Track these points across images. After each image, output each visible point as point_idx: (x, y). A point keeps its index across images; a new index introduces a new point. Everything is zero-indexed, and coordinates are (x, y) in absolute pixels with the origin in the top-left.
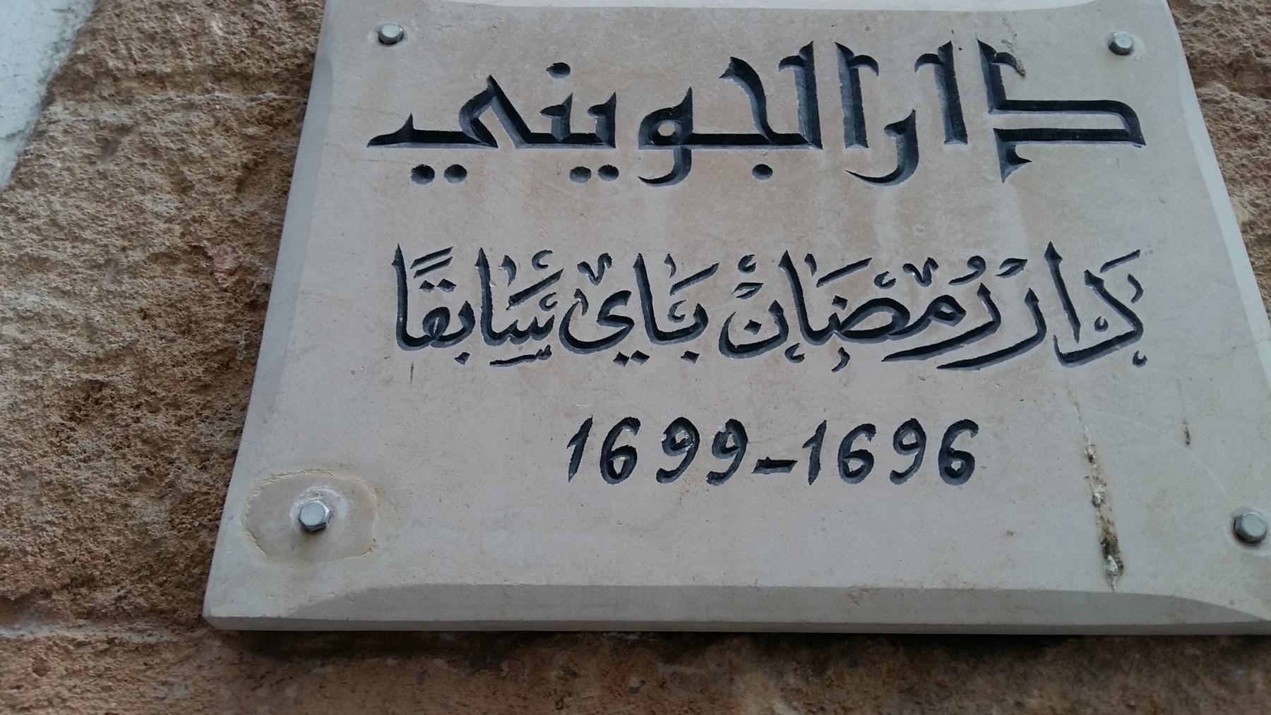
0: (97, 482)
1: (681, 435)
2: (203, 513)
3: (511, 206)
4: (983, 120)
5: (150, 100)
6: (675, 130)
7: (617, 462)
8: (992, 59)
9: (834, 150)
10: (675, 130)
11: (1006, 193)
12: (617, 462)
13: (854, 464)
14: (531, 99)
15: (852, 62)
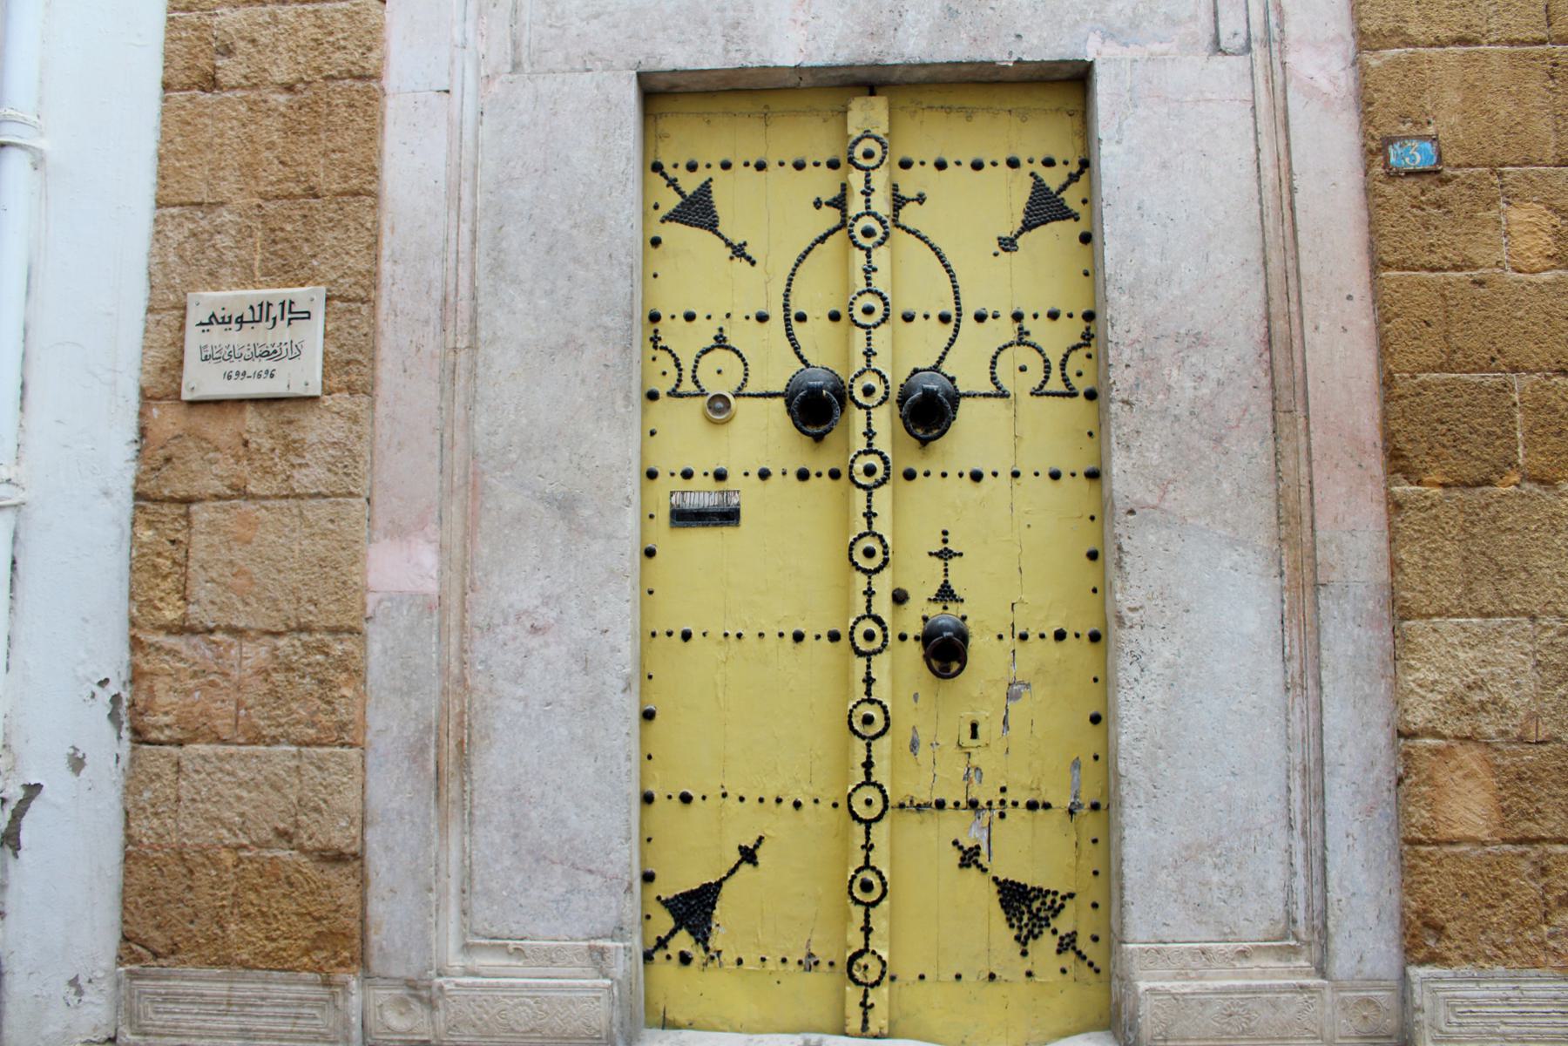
0: (167, 381)
1: (238, 373)
2: (180, 385)
3: (217, 336)
4: (287, 316)
5: (164, 314)
6: (241, 321)
7: (229, 377)
8: (292, 303)
9: (264, 324)
10: (241, 321)
11: (288, 330)
12: (229, 377)
13: (259, 376)
14: (219, 316)
15: (269, 305)
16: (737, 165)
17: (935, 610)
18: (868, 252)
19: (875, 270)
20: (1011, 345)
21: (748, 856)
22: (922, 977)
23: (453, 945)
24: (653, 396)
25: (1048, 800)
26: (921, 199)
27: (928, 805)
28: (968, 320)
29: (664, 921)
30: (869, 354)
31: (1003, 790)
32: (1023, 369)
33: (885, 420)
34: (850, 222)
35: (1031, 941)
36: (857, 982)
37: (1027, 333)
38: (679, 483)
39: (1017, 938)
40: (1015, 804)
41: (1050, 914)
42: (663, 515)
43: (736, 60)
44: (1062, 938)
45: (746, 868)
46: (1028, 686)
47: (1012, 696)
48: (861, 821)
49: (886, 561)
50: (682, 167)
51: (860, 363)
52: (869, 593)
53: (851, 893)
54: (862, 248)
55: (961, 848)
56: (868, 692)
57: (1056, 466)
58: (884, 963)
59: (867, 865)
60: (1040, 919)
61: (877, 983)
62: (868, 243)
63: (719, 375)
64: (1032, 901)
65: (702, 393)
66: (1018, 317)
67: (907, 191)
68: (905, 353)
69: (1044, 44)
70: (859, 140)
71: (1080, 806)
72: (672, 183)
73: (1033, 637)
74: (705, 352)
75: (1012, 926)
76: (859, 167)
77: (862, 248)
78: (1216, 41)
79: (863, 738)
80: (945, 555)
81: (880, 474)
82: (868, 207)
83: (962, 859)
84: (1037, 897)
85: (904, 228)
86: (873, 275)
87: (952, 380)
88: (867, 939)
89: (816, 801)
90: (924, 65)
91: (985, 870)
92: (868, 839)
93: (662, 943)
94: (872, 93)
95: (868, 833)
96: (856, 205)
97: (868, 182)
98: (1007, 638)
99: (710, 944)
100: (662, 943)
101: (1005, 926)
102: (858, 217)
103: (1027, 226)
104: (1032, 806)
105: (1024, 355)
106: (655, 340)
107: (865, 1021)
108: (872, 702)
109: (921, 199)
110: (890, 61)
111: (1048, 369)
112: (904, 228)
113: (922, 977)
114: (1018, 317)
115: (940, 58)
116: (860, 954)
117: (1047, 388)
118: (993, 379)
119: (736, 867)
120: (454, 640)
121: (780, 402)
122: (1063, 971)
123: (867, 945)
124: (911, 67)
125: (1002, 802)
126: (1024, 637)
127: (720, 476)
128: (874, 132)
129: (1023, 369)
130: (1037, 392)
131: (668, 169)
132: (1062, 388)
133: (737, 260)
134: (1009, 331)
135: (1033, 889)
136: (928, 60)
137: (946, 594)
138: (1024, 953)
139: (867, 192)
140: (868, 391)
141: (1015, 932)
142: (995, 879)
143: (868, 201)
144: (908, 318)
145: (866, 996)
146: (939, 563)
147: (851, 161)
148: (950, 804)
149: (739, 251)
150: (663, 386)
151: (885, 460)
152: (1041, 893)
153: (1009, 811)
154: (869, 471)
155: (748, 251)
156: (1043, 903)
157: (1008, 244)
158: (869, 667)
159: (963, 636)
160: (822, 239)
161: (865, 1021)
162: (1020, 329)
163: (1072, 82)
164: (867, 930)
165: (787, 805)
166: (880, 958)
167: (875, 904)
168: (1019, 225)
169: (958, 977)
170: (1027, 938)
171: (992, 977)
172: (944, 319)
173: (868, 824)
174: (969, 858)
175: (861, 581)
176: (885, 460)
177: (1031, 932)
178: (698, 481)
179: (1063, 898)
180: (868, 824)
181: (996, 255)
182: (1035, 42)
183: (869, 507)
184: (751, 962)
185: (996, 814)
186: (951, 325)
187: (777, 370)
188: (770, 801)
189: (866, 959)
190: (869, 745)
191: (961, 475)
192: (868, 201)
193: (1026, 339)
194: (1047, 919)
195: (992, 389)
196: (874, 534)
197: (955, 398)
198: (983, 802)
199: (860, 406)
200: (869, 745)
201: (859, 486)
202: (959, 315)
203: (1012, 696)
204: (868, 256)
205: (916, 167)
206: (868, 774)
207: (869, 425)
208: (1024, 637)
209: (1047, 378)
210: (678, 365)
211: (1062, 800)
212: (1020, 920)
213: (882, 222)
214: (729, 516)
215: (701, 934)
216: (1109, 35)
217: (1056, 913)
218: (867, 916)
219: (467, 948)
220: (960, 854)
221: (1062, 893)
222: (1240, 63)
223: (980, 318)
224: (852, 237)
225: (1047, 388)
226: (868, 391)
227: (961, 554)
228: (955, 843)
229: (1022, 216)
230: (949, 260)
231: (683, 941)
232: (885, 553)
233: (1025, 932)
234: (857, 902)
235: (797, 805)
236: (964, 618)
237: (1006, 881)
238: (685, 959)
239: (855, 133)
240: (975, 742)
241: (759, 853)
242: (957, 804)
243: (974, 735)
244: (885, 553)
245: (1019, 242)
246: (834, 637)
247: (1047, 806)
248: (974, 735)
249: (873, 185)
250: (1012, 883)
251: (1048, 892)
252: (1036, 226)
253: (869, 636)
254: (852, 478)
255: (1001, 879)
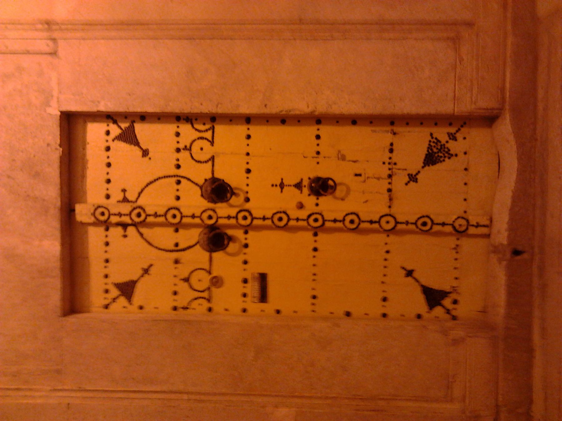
16: (106, 271)
17: (306, 191)
18: (147, 215)
19: (156, 213)
20: (191, 154)
21: (410, 273)
22: (465, 200)
23: (449, 406)
24: (210, 310)
25: (389, 144)
26: (124, 191)
27: (390, 196)
28: (180, 172)
29: (438, 311)
30: (193, 216)
31: (384, 163)
32: (202, 149)
33: (223, 209)
34: (134, 223)
35: (451, 152)
36: (467, 229)
37: (186, 146)
38: (248, 299)
39: (449, 158)
40: (390, 158)
41: (439, 144)
42: (263, 306)
43: (57, 272)
44: (450, 139)
45: (415, 274)
46: (339, 151)
47: (343, 158)
48: (395, 226)
49: (285, 213)
50: (107, 295)
51: (197, 221)
52: (298, 220)
53: (427, 231)
54: (146, 218)
55: (409, 182)
56: (340, 221)
57: (244, 136)
58: (459, 218)
59: (415, 224)
60: (441, 148)
61: (468, 221)
62: (143, 216)
63: (201, 280)
64: (433, 152)
65: (209, 289)
66: (178, 150)
67: (121, 196)
68: (194, 202)
69: (52, 134)
70: (95, 217)
71: (392, 130)
72: (114, 300)
73: (318, 149)
74: (191, 287)
75: (444, 160)
76: (109, 218)
77: (146, 218)
78: (50, 54)
79: (359, 224)
80: (282, 186)
81: (247, 214)
82: (127, 215)
83: (414, 181)
84: (432, 150)
85: (137, 199)
86: (158, 214)
87: (206, 180)
88: (447, 224)
89: (386, 244)
90: (61, 188)
91: (419, 172)
92: (403, 223)
93: (448, 311)
94: (74, 210)
95: (401, 223)
96: (127, 220)
97: (115, 215)
98: (318, 160)
99: (448, 291)
100: (448, 311)
101: (444, 163)
102: (131, 219)
103: (137, 144)
104: (391, 151)
105: (195, 148)
106: (185, 308)
107: (484, 226)
108: (344, 220)
109: (124, 191)
110: (59, 204)
111: (202, 138)
112: (137, 199)
113: (465, 200)
114: (178, 150)
115: (57, 180)
116: (454, 228)
117: (210, 139)
118: (206, 162)
119: (415, 278)
120: (316, 401)
121: (215, 255)
122: (465, 138)
123: (450, 225)
124: (62, 195)
125: (389, 164)
126: (318, 153)
127: (245, 281)
128: (92, 211)
129: (202, 149)
130: (212, 143)
131: (107, 302)
132: (210, 133)
133: (149, 272)
134: (184, 155)
135: (428, 151)
136: (59, 187)
137: (299, 186)
138: (456, 155)
139: (120, 215)
140: (210, 217)
141: (446, 159)
142: (423, 167)
143: (124, 215)
144: (178, 198)
145: (473, 226)
146: (285, 189)
147: (106, 222)
148: (390, 186)
149: (146, 271)
150: (206, 305)
151: (240, 211)
152: (430, 147)
153: (394, 160)
154: (245, 218)
155: (146, 267)
156: (435, 147)
157: (145, 153)
158: (329, 221)
159: (318, 179)
160: (141, 235)
161: (484, 226)
162: (184, 149)
163: (71, 122)
164: (443, 224)
165: (387, 256)
166: (456, 219)
167: (432, 221)
168: (137, 148)
169: (466, 184)
170: (449, 154)
171: (466, 169)
172: (179, 182)
173: (397, 223)
174: (413, 178)
175: (292, 223)
176: (240, 211)
177: (447, 152)
178: (248, 291)
179: (432, 138)
180: (397, 223)
181: (150, 158)
182: (50, 138)
183: (260, 218)
184: (456, 273)
185: (394, 166)
186: (182, 180)
187: (200, 256)
188: (386, 263)
189: (457, 225)
190: (363, 222)
191: (248, 178)
192: (124, 215)
193: (188, 147)
194: (441, 145)
195: (210, 163)
196: (272, 217)
197: (214, 180)
198: (390, 172)
199: (217, 221)
200: (363, 222)
201: (252, 222)
202: (177, 176)
203: (343, 158)
204: (150, 215)
205: (109, 192)
206: (375, 222)
207: (225, 218)
208: (318, 153)
209: (206, 139)
210: (196, 299)
211: (389, 138)
212: (441, 157)
213: (134, 209)
214: (263, 278)
215: (444, 294)
216: (47, 104)
217: (439, 141)
218: (437, 224)
219: (452, 401)
220: (411, 182)
221: (430, 138)
222: (61, 43)
223: (178, 167)
224: (141, 222)
225: (210, 139)
226: (210, 217)
227: (282, 179)
228: (406, 184)
229: (133, 146)
230: (152, 179)
231: (447, 302)
232: (281, 212)
233: (446, 155)
234: (431, 228)
235: (388, 252)
236: (309, 178)
237: (424, 163)
238: (455, 302)
239: (92, 220)
240: (363, 175)
241: (409, 268)
242: (390, 183)
243: (360, 175)
244: (281, 212)
245: (144, 148)
246: (316, 235)
247: (392, 144)
248: (360, 175)
249: (117, 212)
250: (425, 160)
251: (429, 145)
252: (137, 140)
253: (316, 220)
254: (248, 226)
255: (422, 165)
